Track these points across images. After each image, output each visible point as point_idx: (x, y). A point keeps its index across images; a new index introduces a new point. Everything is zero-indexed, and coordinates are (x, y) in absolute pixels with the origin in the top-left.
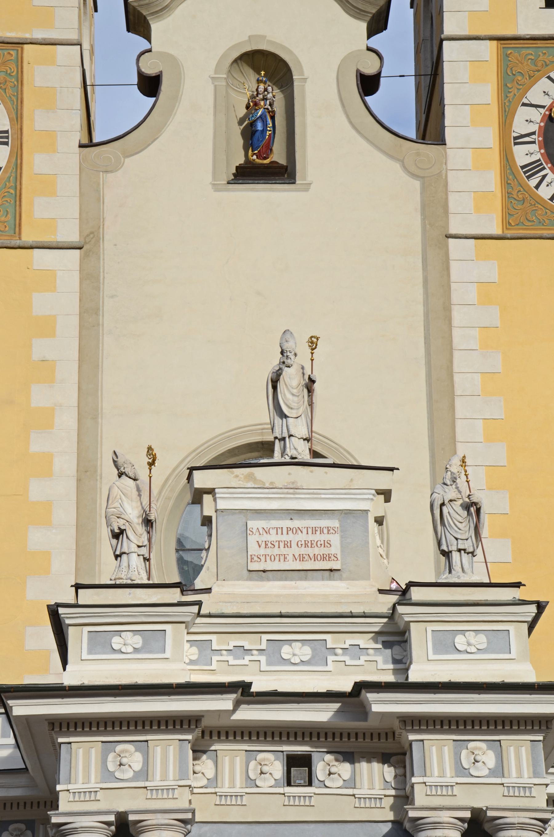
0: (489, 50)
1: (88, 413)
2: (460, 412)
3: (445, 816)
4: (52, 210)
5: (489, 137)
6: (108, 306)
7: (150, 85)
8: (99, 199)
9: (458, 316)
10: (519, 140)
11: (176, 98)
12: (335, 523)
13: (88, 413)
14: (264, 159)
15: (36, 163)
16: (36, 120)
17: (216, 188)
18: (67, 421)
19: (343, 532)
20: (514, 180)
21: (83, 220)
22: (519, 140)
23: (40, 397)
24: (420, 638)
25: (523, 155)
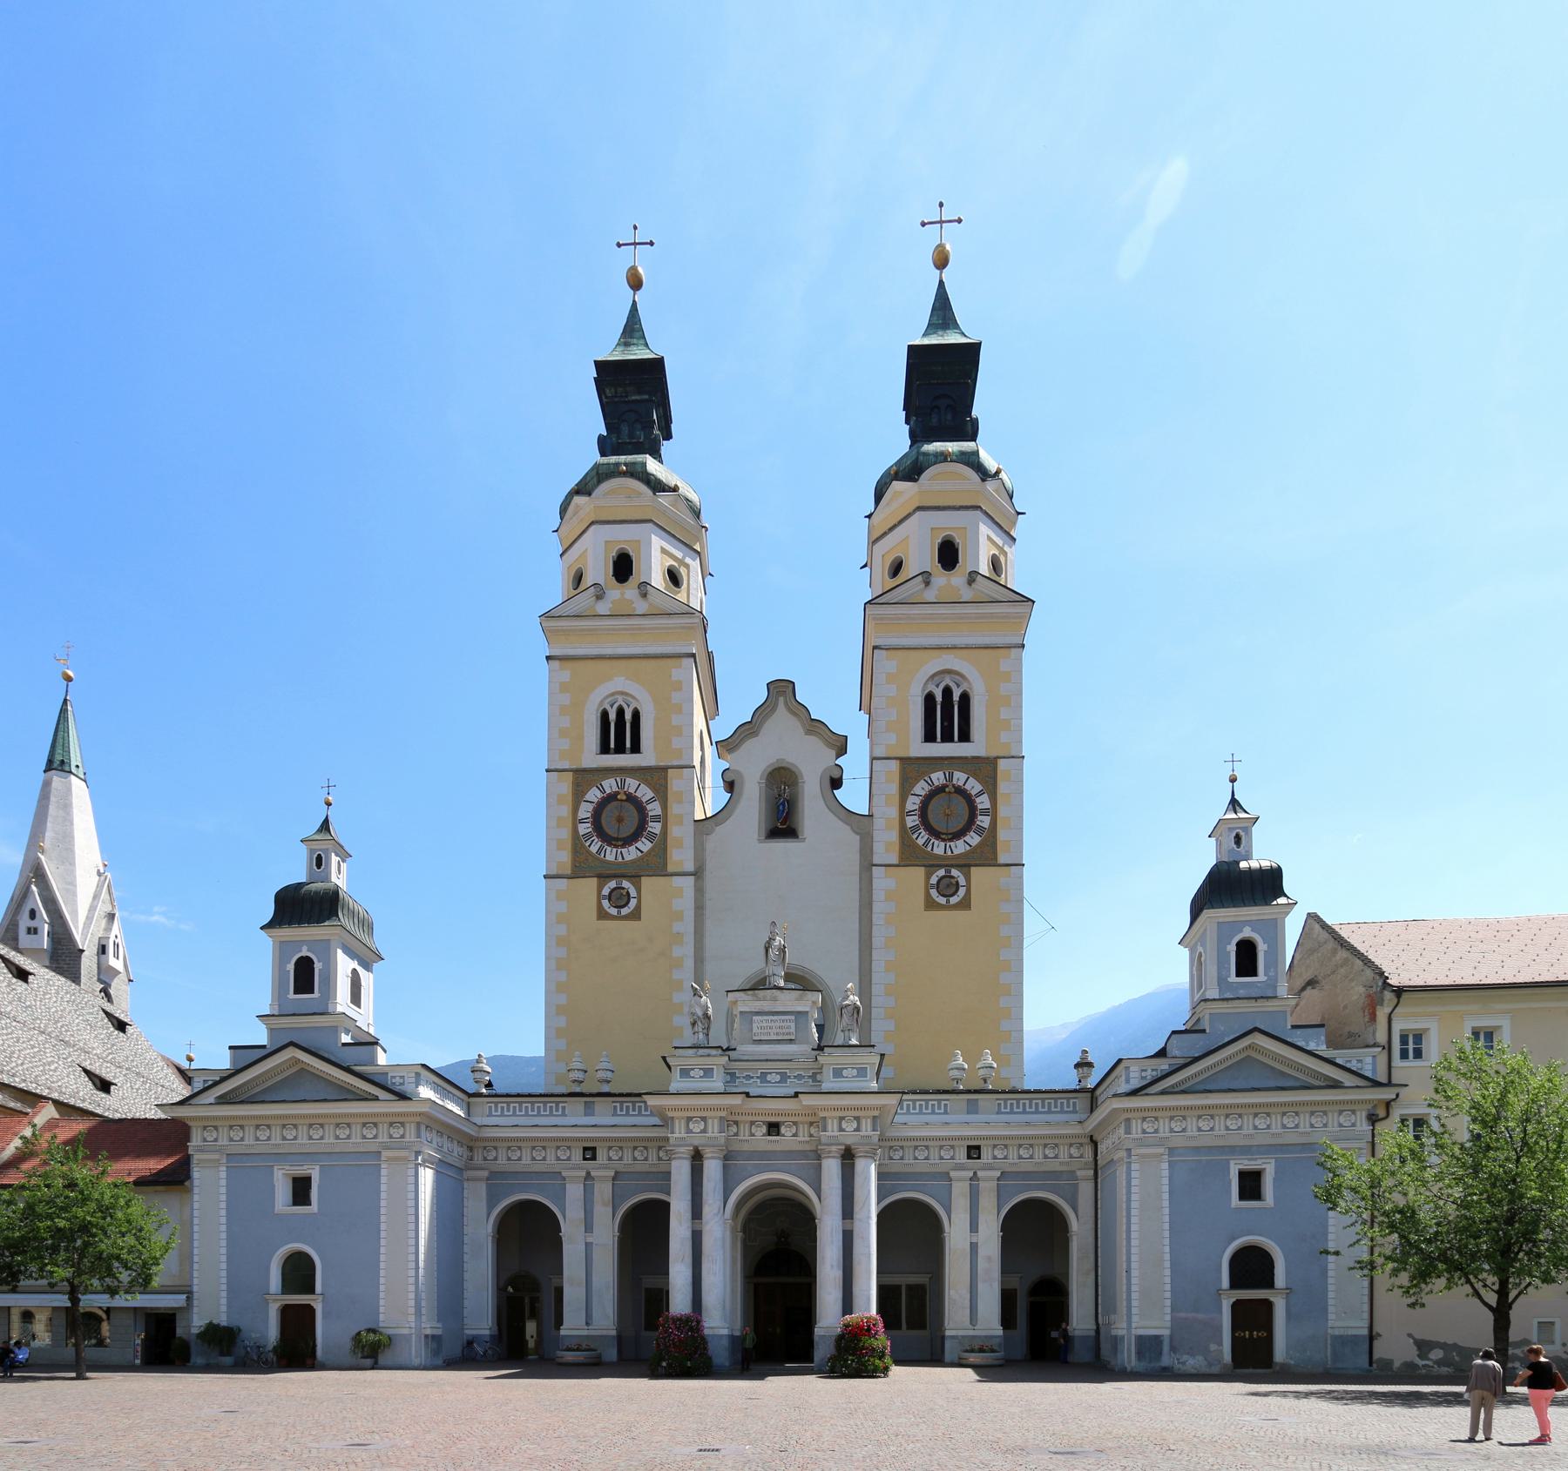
0: (894, 766)
2: (874, 957)
4: (681, 856)
5: (894, 812)
6: (708, 904)
7: (730, 786)
8: (703, 850)
9: (876, 907)
10: (909, 813)
11: (741, 794)
14: (782, 823)
15: (675, 831)
16: (674, 809)
17: (760, 841)
20: (905, 833)
21: (696, 859)
22: (909, 813)
24: (828, 1074)
25: (909, 824)
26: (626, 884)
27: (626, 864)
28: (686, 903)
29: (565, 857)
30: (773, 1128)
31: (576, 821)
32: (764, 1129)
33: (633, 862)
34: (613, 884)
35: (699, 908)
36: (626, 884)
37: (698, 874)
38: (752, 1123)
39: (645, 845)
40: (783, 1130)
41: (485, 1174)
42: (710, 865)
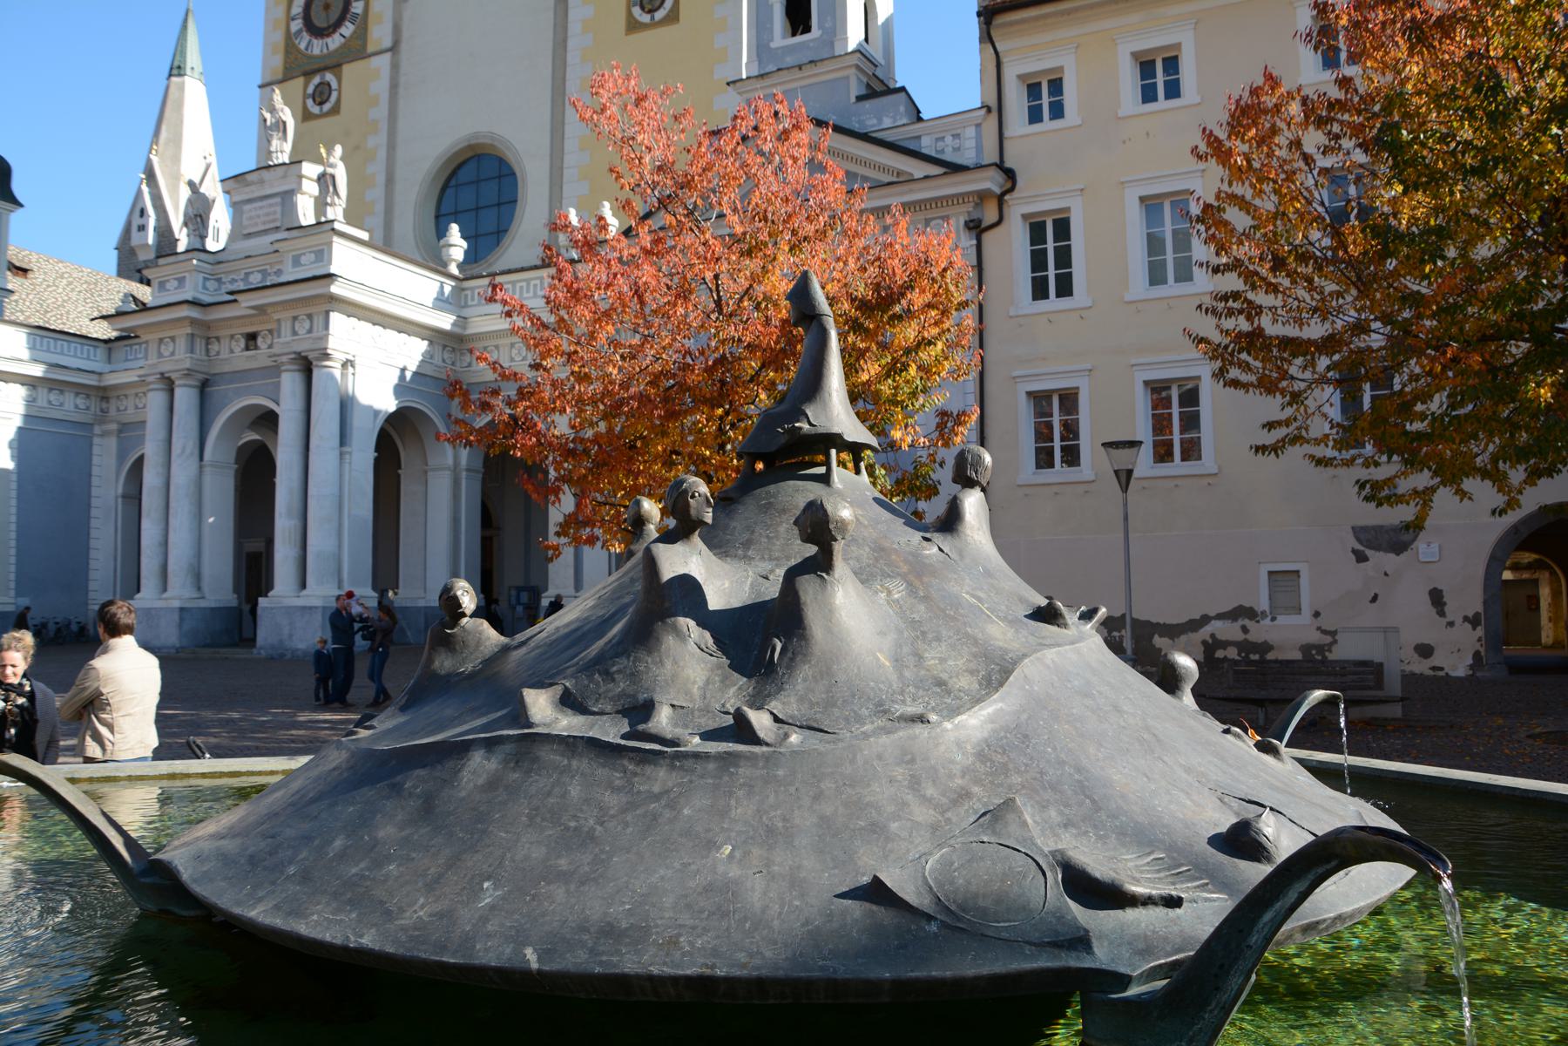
1: (392, 147)
3: (284, 359)
6: (402, 80)
9: (571, 43)
12: (278, 200)
13: (392, 147)
18: (382, 154)
19: (283, 204)
23: (371, 142)
26: (329, 77)
27: (330, 55)
28: (381, 87)
29: (278, 61)
30: (252, 338)
31: (290, 19)
32: (242, 343)
33: (336, 50)
34: (317, 80)
35: (394, 86)
36: (329, 77)
37: (394, 49)
38: (232, 337)
39: (348, 29)
40: (260, 340)
41: (114, 427)
42: (405, 34)
